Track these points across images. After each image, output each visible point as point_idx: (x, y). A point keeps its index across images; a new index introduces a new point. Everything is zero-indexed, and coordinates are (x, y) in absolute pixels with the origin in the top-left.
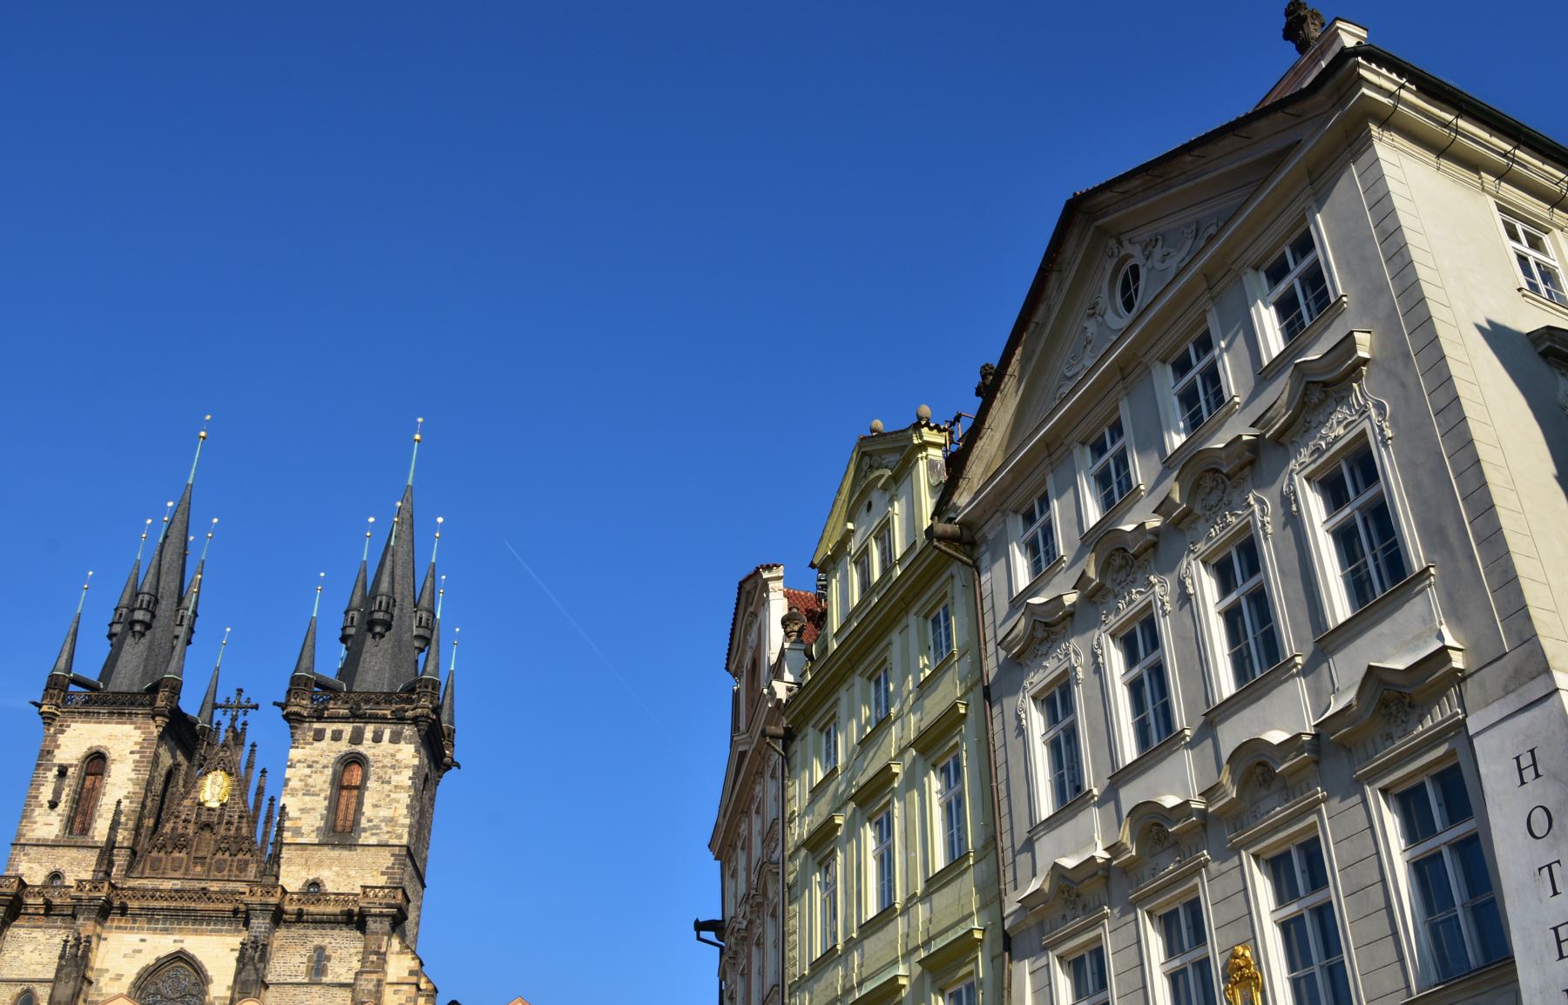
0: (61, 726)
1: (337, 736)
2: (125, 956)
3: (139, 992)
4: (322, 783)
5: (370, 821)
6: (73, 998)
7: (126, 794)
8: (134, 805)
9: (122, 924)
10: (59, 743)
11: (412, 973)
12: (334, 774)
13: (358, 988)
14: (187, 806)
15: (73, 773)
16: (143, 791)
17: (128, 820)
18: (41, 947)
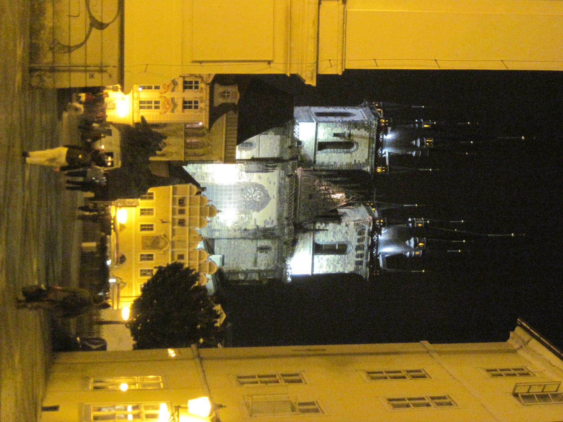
1: (359, 240)
2: (268, 178)
5: (322, 258)
9: (281, 174)
10: (361, 130)
16: (337, 169)
18: (272, 146)
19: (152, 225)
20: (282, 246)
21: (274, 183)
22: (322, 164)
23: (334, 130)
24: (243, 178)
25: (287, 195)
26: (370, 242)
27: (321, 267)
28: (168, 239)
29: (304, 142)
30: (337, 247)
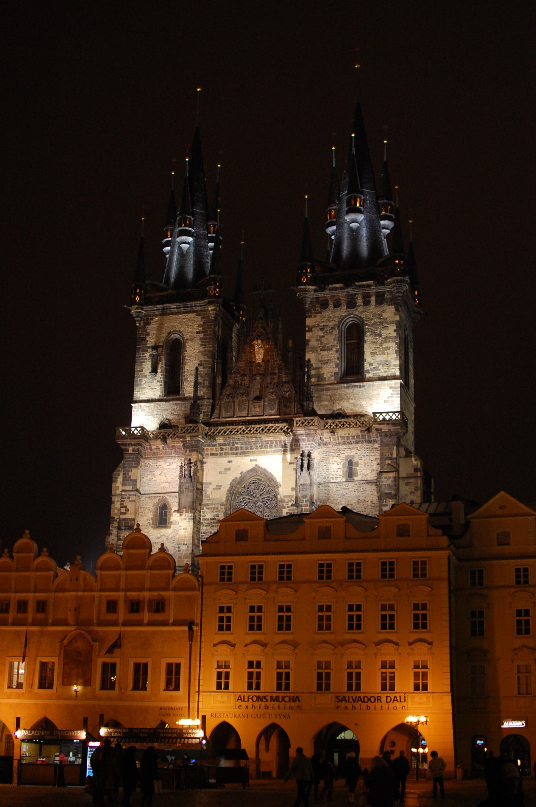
0: (147, 319)
1: (337, 305)
2: (220, 473)
3: (233, 496)
4: (332, 341)
5: (371, 365)
6: (193, 504)
7: (199, 363)
8: (206, 370)
9: (214, 452)
10: (148, 331)
11: (416, 470)
12: (340, 332)
13: (381, 484)
14: (243, 367)
15: (162, 352)
17: (204, 380)
19: (43, 665)
20: (342, 437)
21: (230, 462)
22: (196, 384)
23: (146, 374)
24: (218, 516)
25: (247, 437)
26: (338, 286)
27: (386, 364)
28: (71, 631)
29: (162, 419)
30: (353, 341)
